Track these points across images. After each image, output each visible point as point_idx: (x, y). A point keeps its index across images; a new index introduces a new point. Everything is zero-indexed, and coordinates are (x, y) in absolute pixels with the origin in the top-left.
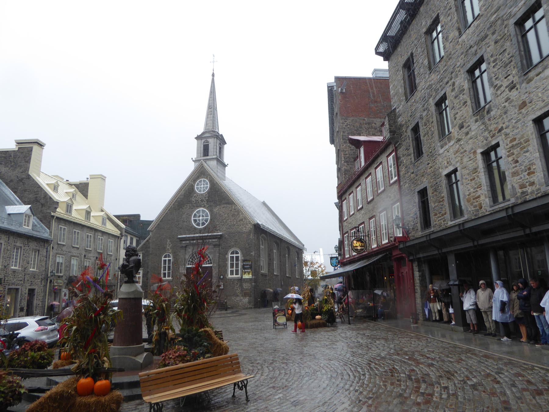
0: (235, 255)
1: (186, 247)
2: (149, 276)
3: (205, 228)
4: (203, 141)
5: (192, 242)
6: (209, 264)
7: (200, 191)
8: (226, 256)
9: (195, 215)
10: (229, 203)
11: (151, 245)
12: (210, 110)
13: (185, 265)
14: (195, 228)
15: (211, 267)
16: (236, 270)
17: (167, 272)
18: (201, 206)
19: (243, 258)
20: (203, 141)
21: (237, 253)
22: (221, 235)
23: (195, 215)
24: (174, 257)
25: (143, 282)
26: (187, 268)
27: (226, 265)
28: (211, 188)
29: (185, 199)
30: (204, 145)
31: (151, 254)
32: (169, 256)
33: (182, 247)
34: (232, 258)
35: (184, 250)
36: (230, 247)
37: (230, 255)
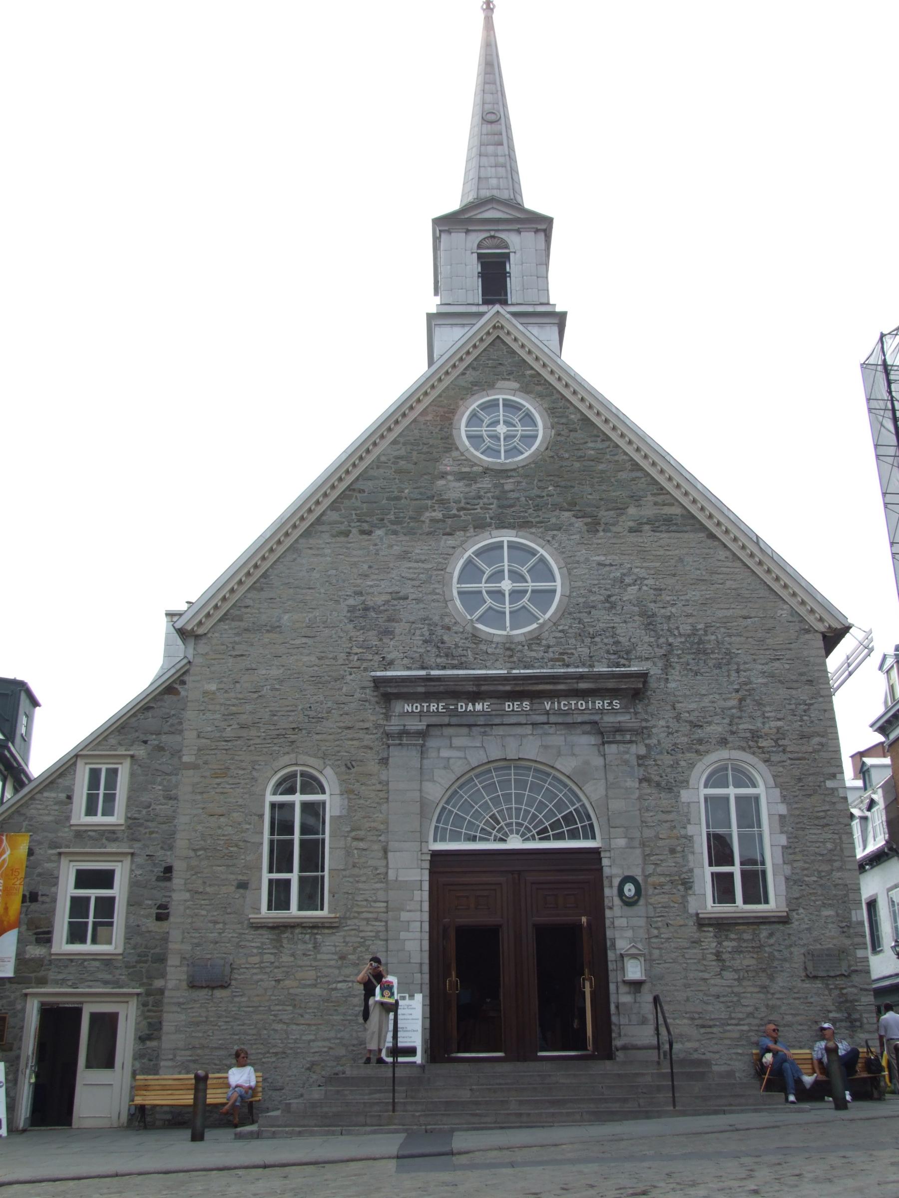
0: (732, 792)
1: (423, 734)
2: (179, 896)
3: (535, 640)
4: (475, 238)
5: (462, 706)
6: (574, 835)
7: (493, 451)
8: (685, 795)
9: (469, 562)
10: (666, 523)
11: (190, 714)
12: (487, 128)
13: (423, 841)
14: (475, 638)
15: (595, 853)
16: (744, 874)
17: (294, 877)
18: (502, 525)
19: (783, 809)
20: (475, 238)
21: (744, 779)
22: (644, 676)
23: (471, 571)
24: (347, 792)
25: (132, 931)
26: (435, 854)
27: (680, 846)
28: (552, 446)
29: (392, 488)
30: (480, 256)
31: (195, 767)
32: (312, 784)
33: (404, 733)
34: (717, 805)
35: (414, 753)
36: (699, 747)
37: (704, 791)
